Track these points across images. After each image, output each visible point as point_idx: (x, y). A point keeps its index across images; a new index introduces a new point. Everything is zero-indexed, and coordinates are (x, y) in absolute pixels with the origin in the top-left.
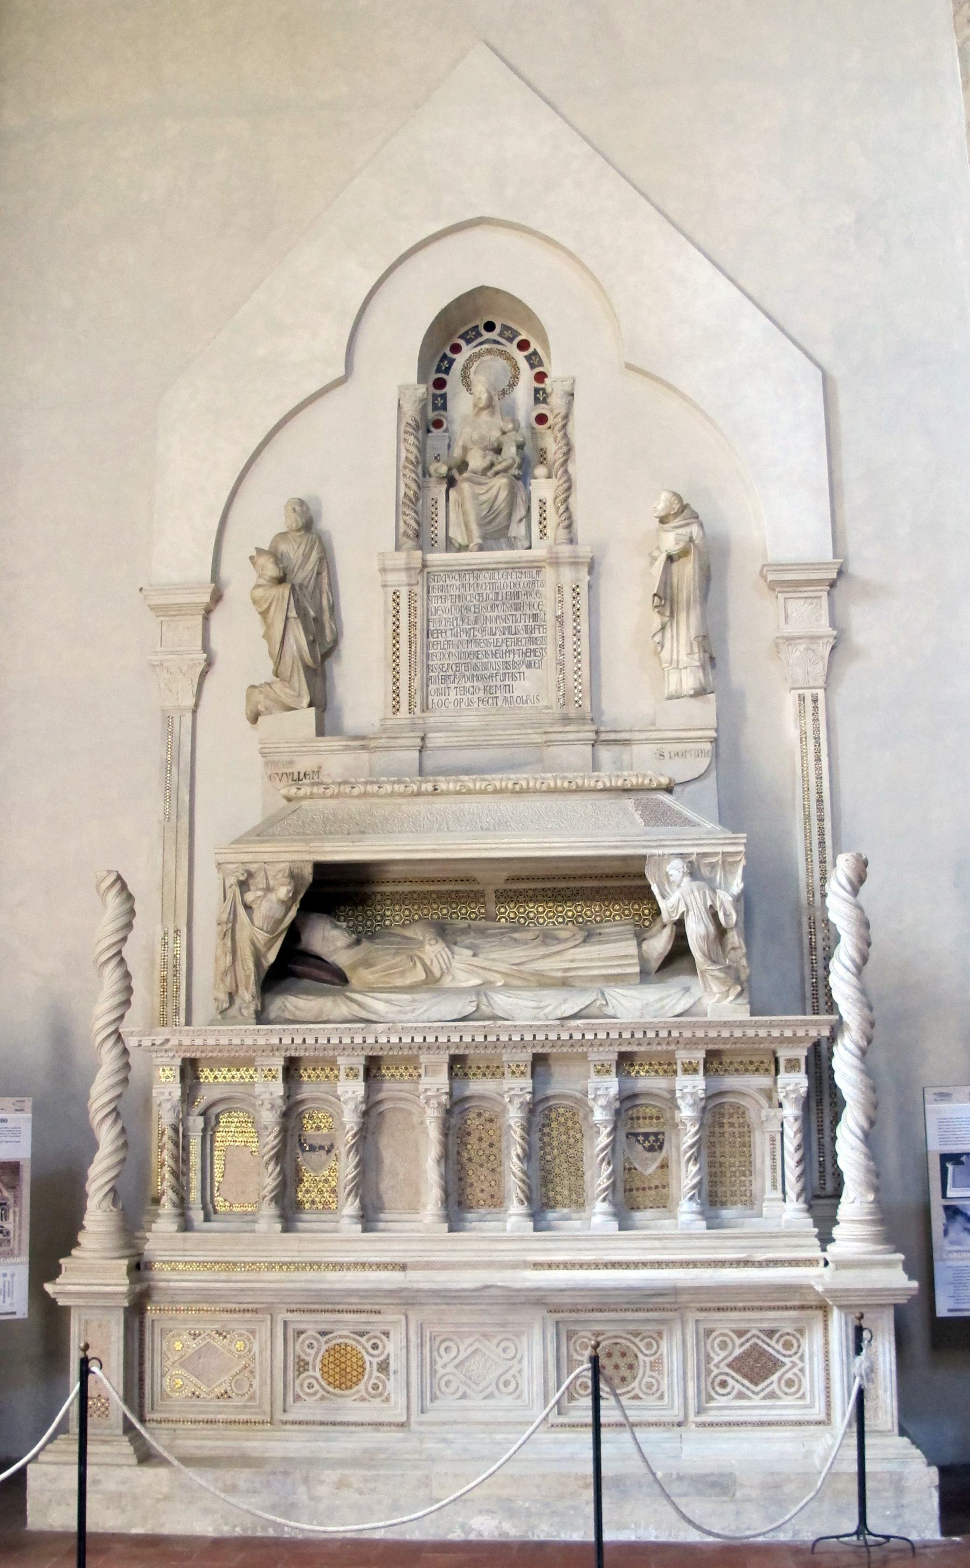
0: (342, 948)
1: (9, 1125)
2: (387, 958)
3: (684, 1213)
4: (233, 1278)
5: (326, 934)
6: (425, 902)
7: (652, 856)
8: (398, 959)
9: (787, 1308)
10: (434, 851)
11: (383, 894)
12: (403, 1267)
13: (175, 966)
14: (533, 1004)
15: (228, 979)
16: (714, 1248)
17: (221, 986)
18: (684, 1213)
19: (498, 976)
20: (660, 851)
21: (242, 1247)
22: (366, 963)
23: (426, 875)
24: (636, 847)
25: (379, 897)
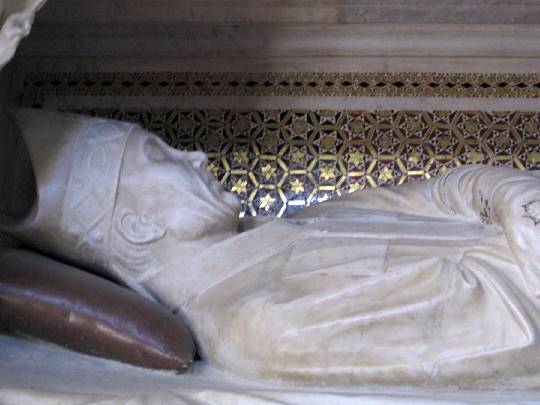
0: (186, 236)
2: (358, 268)
5: (131, 181)
6: (445, 143)
8: (408, 270)
11: (313, 117)
22: (283, 286)
23: (447, 68)
25: (300, 127)
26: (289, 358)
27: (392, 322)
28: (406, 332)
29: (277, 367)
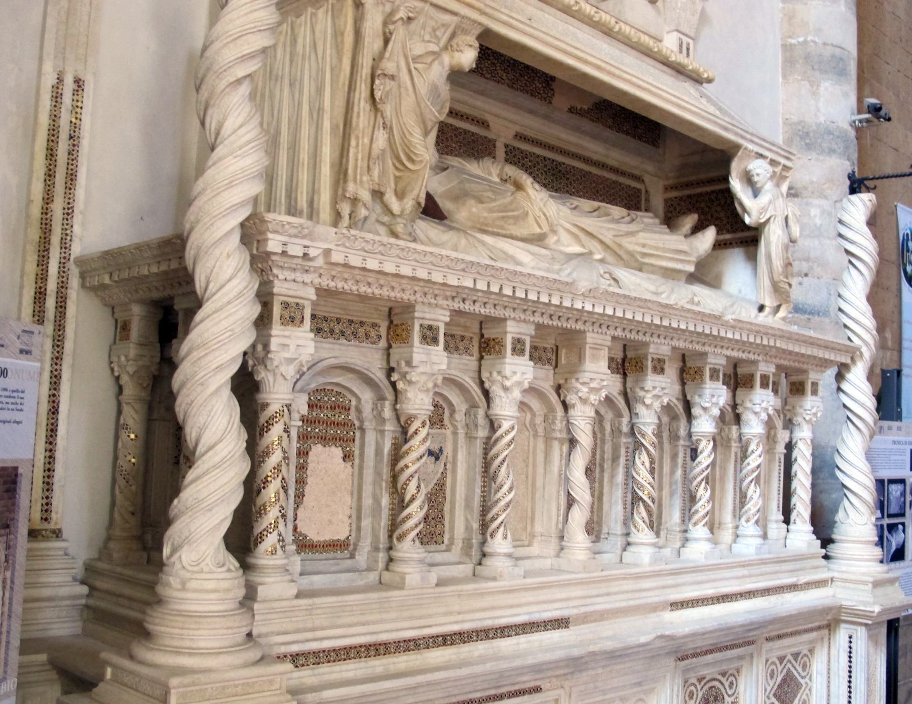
1: (10, 382)
3: (752, 536)
4: (392, 669)
7: (746, 149)
9: (806, 631)
10: (599, 68)
12: (561, 623)
13: (71, 138)
14: (652, 288)
15: (376, 173)
16: (776, 573)
17: (365, 178)
18: (752, 536)
19: (599, 246)
20: (750, 146)
21: (393, 615)
24: (736, 134)
26: (483, 224)
27: (509, 217)
28: (511, 221)
29: (479, 226)
